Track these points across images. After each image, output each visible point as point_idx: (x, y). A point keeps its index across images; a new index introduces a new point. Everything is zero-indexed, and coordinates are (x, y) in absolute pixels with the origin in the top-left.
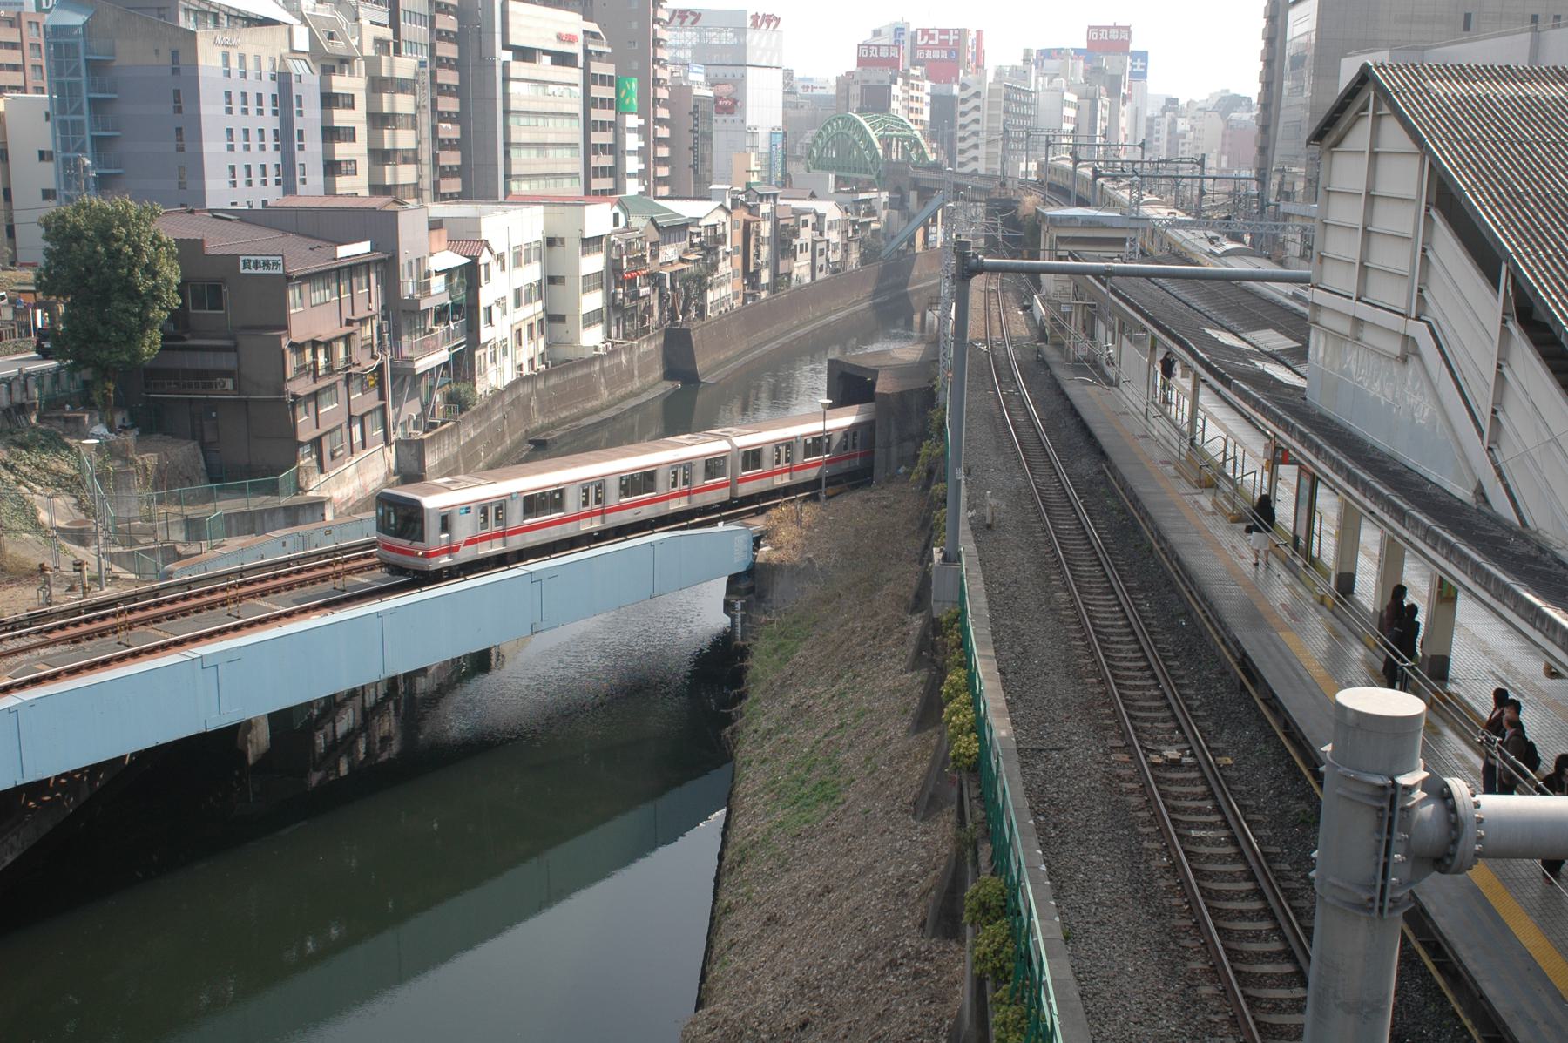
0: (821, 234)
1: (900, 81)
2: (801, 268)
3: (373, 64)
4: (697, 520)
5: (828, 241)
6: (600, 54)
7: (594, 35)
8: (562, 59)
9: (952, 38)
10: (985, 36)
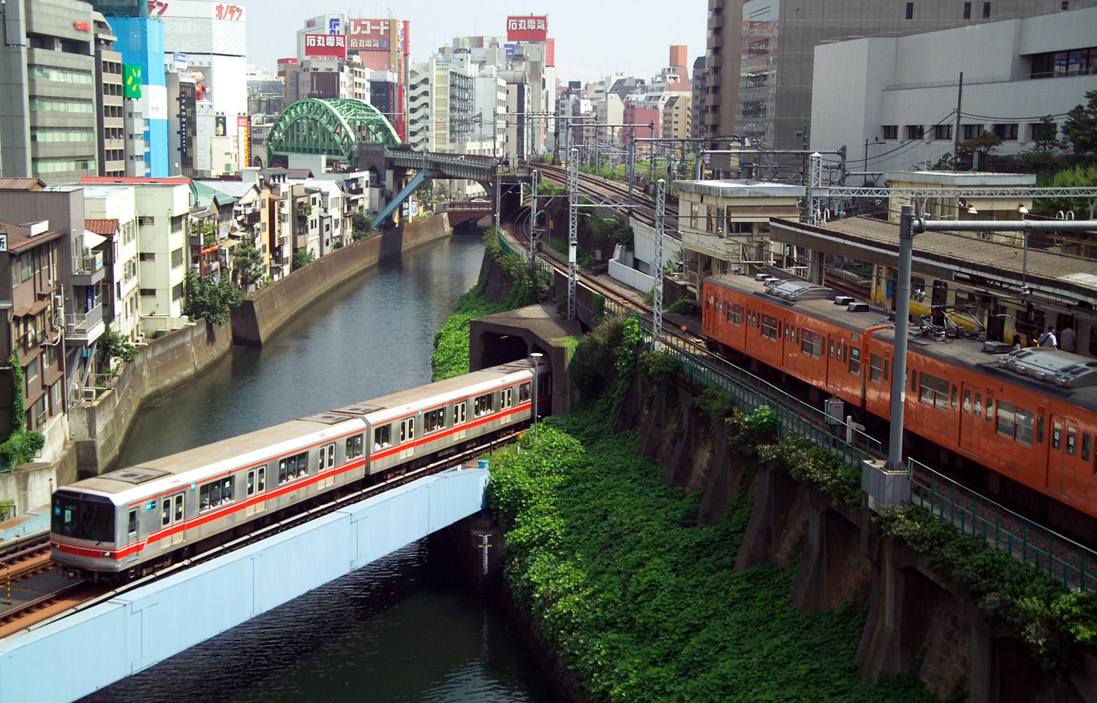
0: (325, 211)
1: (346, 68)
2: (311, 242)
4: (432, 465)
5: (331, 217)
6: (108, 42)
7: (100, 24)
9: (383, 28)
10: (410, 26)
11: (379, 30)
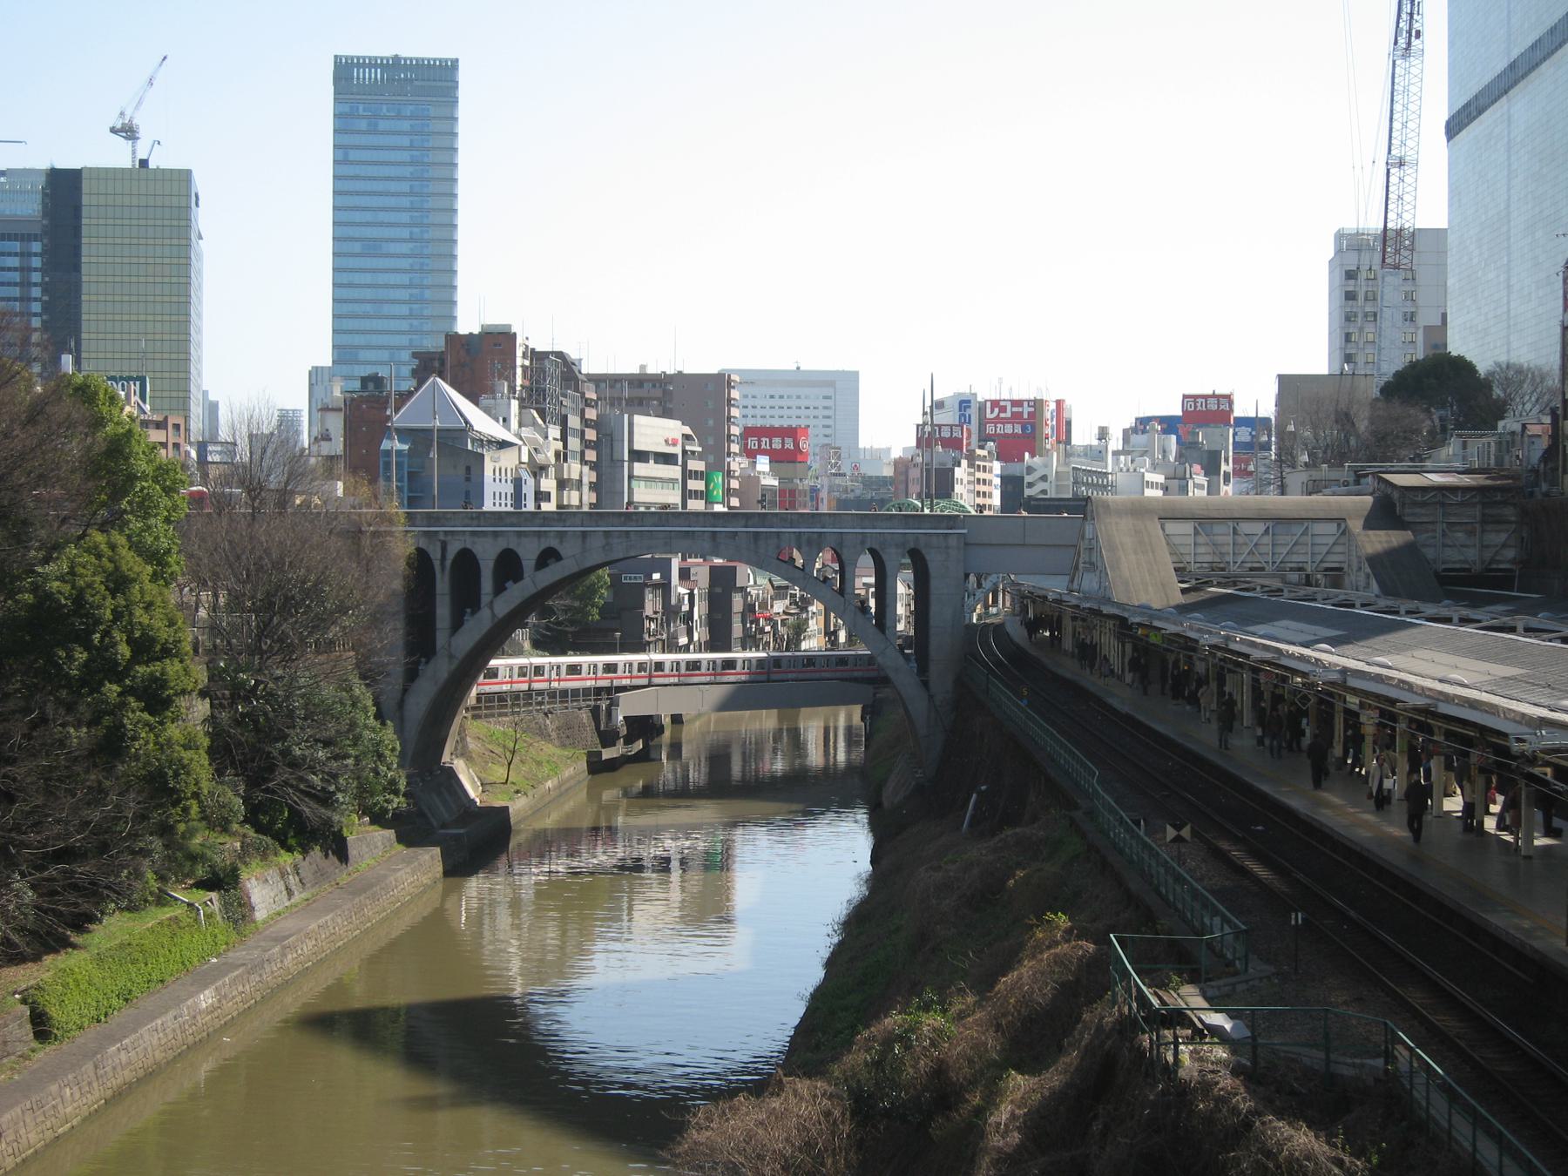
1: (964, 463)
3: (559, 470)
6: (693, 452)
7: (686, 437)
9: (1026, 410)
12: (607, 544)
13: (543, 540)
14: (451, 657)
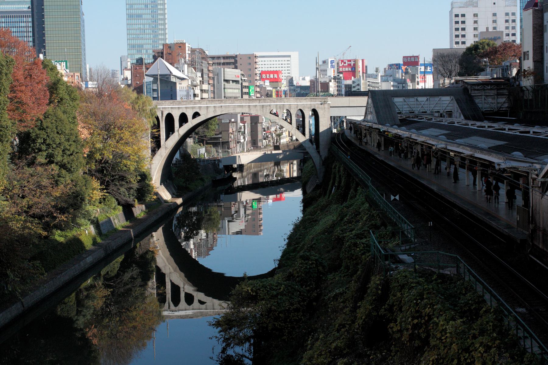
3: (201, 87)
7: (243, 75)
8: (237, 82)
9: (352, 63)
11: (351, 64)
12: (215, 110)
13: (194, 109)
14: (166, 148)
